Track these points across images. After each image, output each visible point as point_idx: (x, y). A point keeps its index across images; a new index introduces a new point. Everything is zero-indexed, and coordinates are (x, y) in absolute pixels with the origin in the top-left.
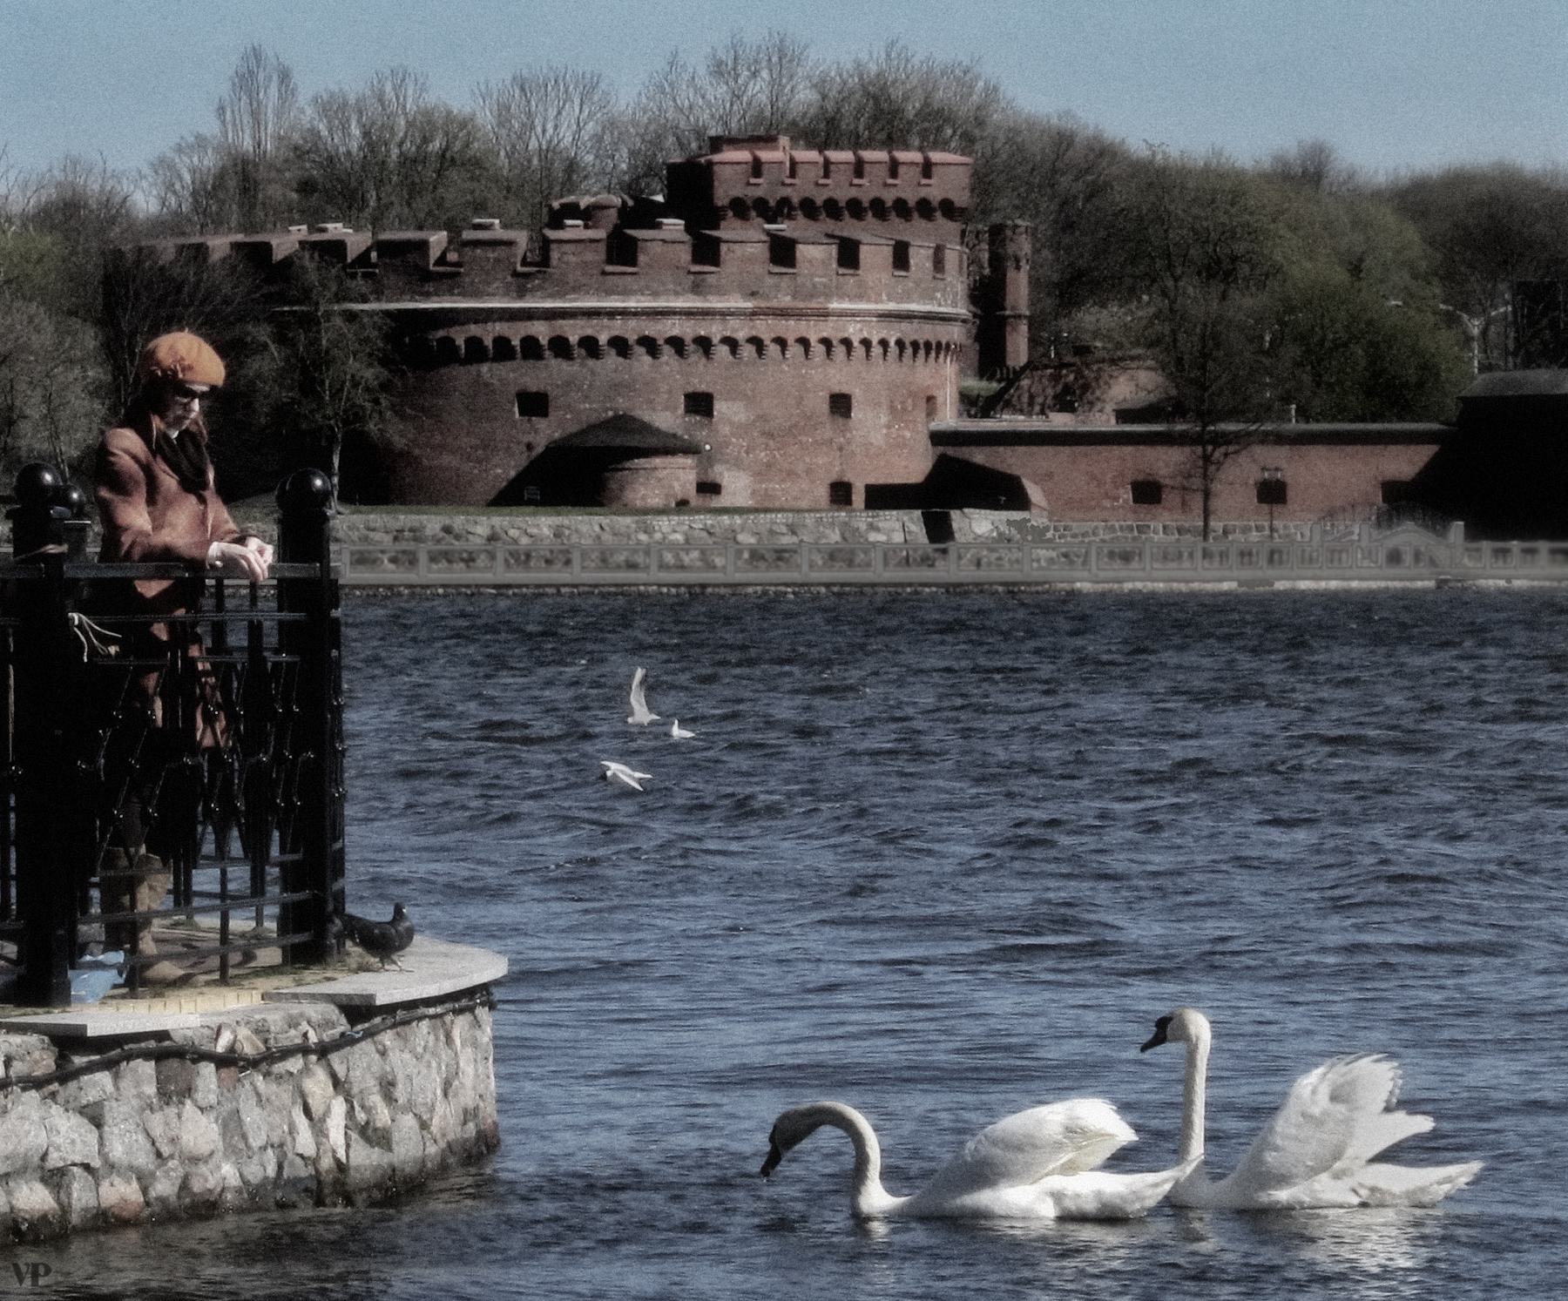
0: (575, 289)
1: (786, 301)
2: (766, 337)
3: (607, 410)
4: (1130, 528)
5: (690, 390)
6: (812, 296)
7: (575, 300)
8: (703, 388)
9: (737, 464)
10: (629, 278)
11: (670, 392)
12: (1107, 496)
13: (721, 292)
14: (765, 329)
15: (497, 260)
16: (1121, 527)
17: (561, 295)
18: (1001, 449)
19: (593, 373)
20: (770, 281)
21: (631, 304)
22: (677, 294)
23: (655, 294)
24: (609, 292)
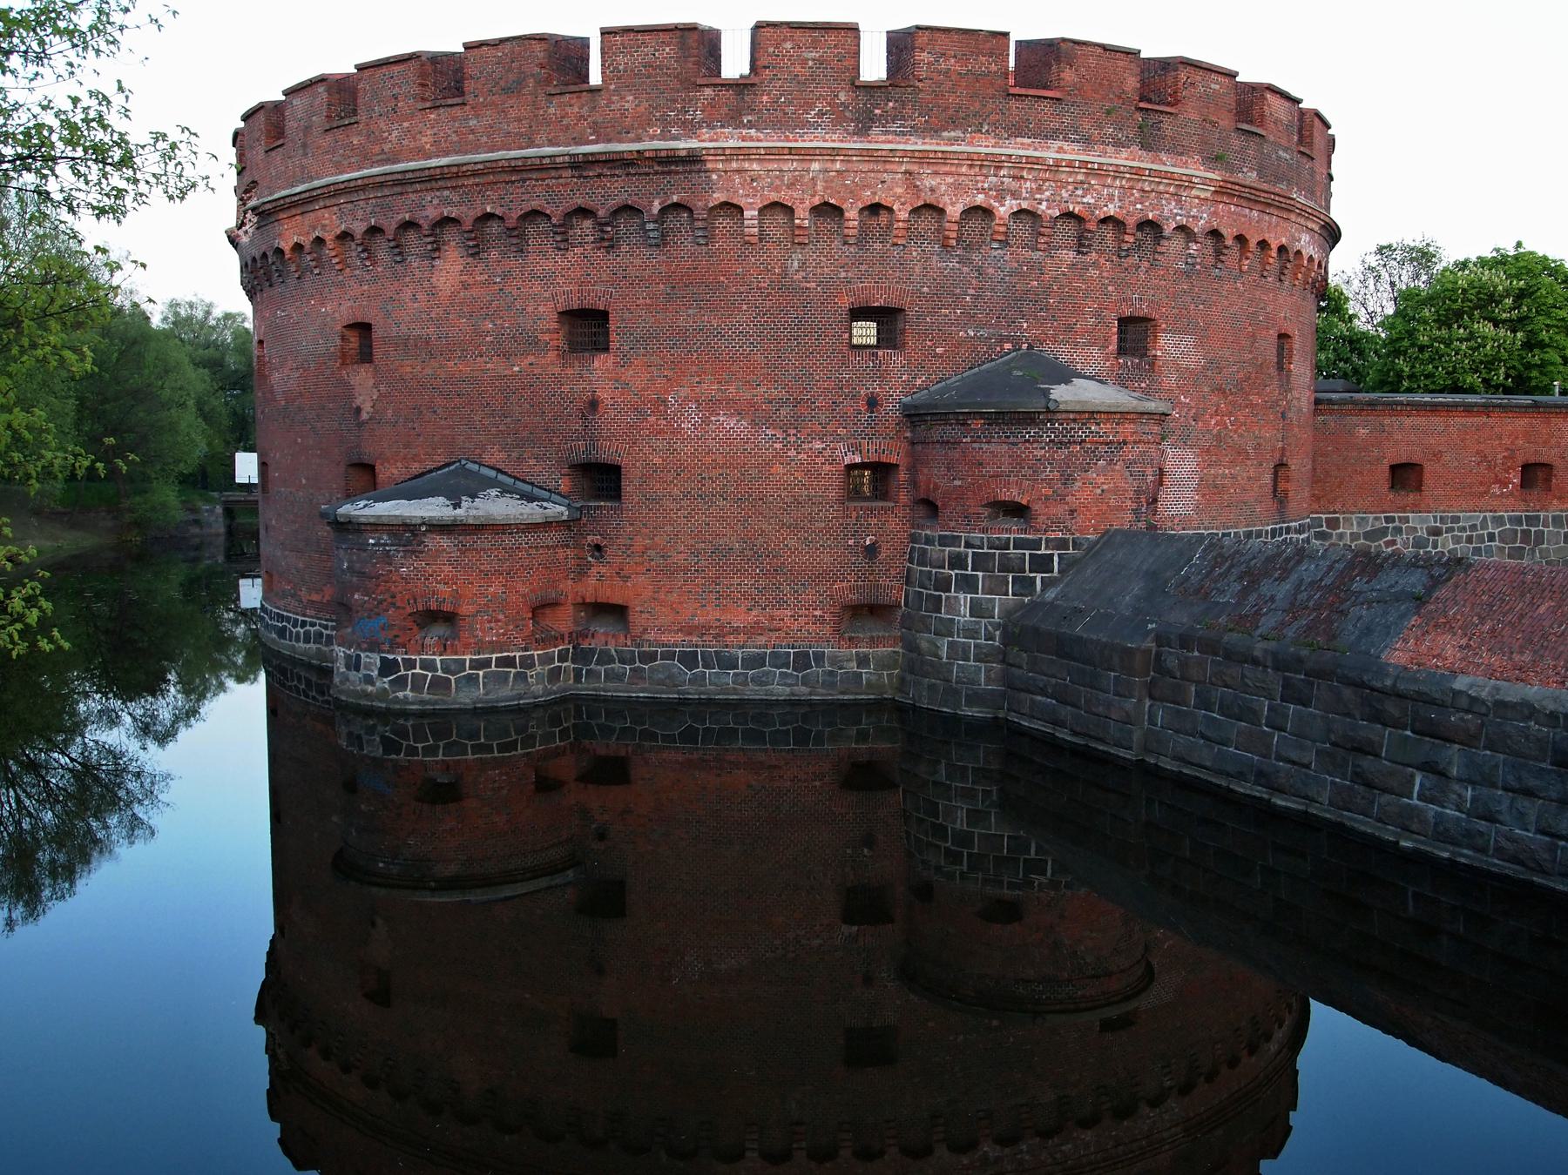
0: (953, 123)
1: (1251, 177)
2: (1228, 233)
3: (1002, 340)
4: (1518, 521)
5: (1127, 314)
6: (1278, 179)
7: (956, 139)
8: (1144, 310)
9: (1184, 441)
10: (1045, 107)
11: (1097, 315)
12: (1497, 481)
13: (1178, 150)
14: (1231, 218)
15: (820, 62)
16: (1510, 518)
17: (933, 131)
18: (1387, 421)
19: (980, 271)
20: (1236, 142)
21: (1050, 153)
22: (1118, 144)
23: (1087, 142)
24: (1017, 130)
